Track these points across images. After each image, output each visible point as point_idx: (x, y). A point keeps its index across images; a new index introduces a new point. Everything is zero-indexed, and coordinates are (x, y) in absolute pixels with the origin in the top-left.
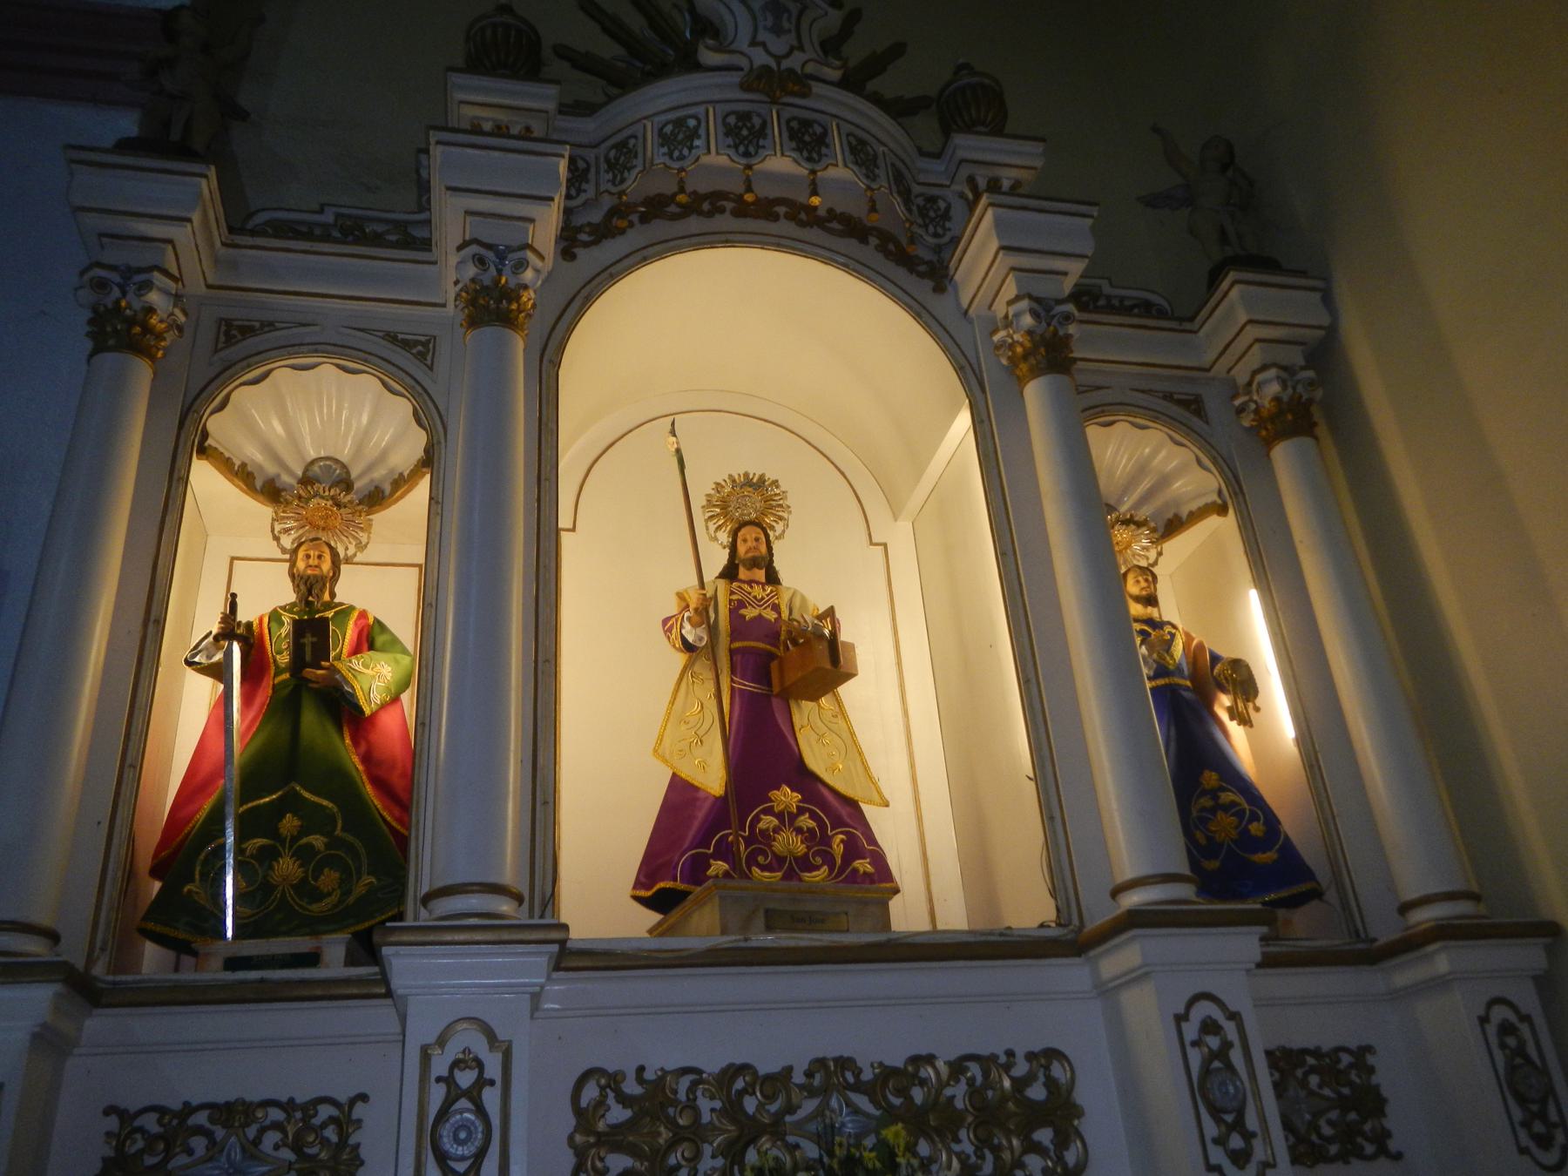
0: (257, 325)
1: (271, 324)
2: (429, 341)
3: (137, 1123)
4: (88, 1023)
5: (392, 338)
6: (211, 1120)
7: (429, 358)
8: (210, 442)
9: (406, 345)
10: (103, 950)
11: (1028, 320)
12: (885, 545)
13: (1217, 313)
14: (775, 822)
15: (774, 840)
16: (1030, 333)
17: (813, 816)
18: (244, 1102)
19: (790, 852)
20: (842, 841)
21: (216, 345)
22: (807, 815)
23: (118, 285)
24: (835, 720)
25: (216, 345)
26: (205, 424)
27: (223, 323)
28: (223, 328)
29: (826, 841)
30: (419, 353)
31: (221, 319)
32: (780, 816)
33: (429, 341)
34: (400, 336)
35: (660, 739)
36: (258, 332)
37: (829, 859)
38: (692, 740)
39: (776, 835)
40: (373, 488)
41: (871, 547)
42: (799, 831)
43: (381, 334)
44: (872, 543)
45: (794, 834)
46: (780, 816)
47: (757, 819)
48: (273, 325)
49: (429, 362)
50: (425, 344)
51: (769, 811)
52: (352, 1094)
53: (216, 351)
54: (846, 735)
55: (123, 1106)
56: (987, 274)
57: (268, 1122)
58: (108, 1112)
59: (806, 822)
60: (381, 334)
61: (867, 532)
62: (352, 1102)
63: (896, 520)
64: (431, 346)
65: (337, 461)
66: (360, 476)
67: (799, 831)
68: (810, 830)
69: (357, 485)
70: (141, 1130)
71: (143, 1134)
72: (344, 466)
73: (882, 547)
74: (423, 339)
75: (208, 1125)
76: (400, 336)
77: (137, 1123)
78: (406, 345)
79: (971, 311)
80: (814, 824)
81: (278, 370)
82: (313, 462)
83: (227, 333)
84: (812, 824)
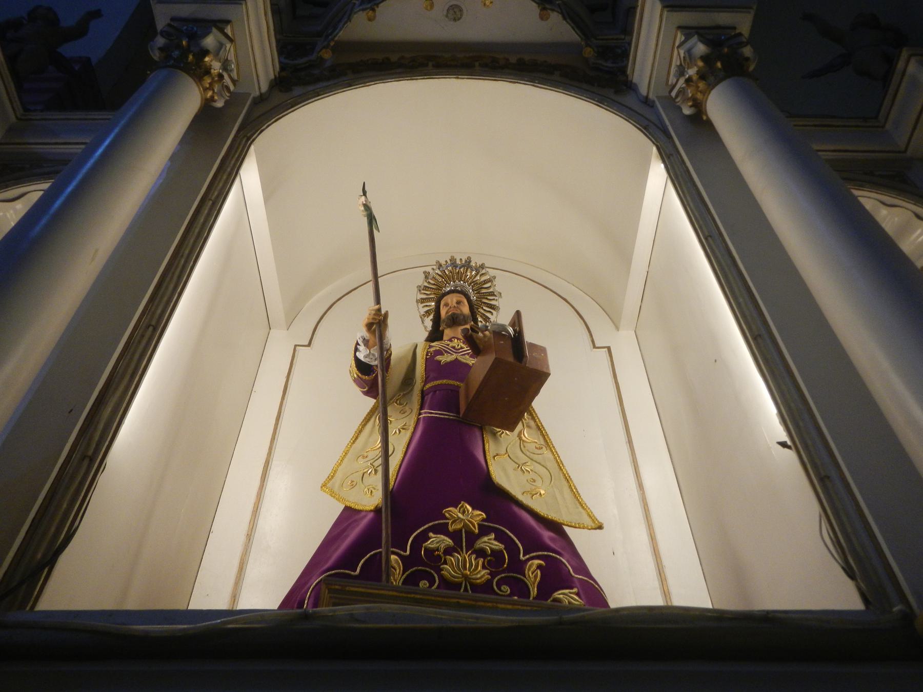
11: (701, 48)
12: (609, 348)
13: (899, 96)
14: (449, 541)
15: (445, 563)
16: (704, 58)
17: (500, 537)
19: (466, 577)
20: (539, 567)
22: (493, 536)
24: (539, 451)
29: (518, 566)
32: (455, 536)
35: (331, 477)
37: (521, 589)
38: (366, 470)
39: (448, 557)
41: (595, 350)
42: (481, 553)
44: (595, 347)
45: (474, 556)
46: (455, 536)
47: (424, 537)
51: (442, 529)
54: (552, 465)
56: (657, 41)
59: (489, 542)
61: (590, 339)
63: (618, 330)
67: (481, 553)
68: (496, 554)
73: (606, 349)
79: (651, 96)
80: (502, 546)
81: (34, 193)
84: (498, 546)
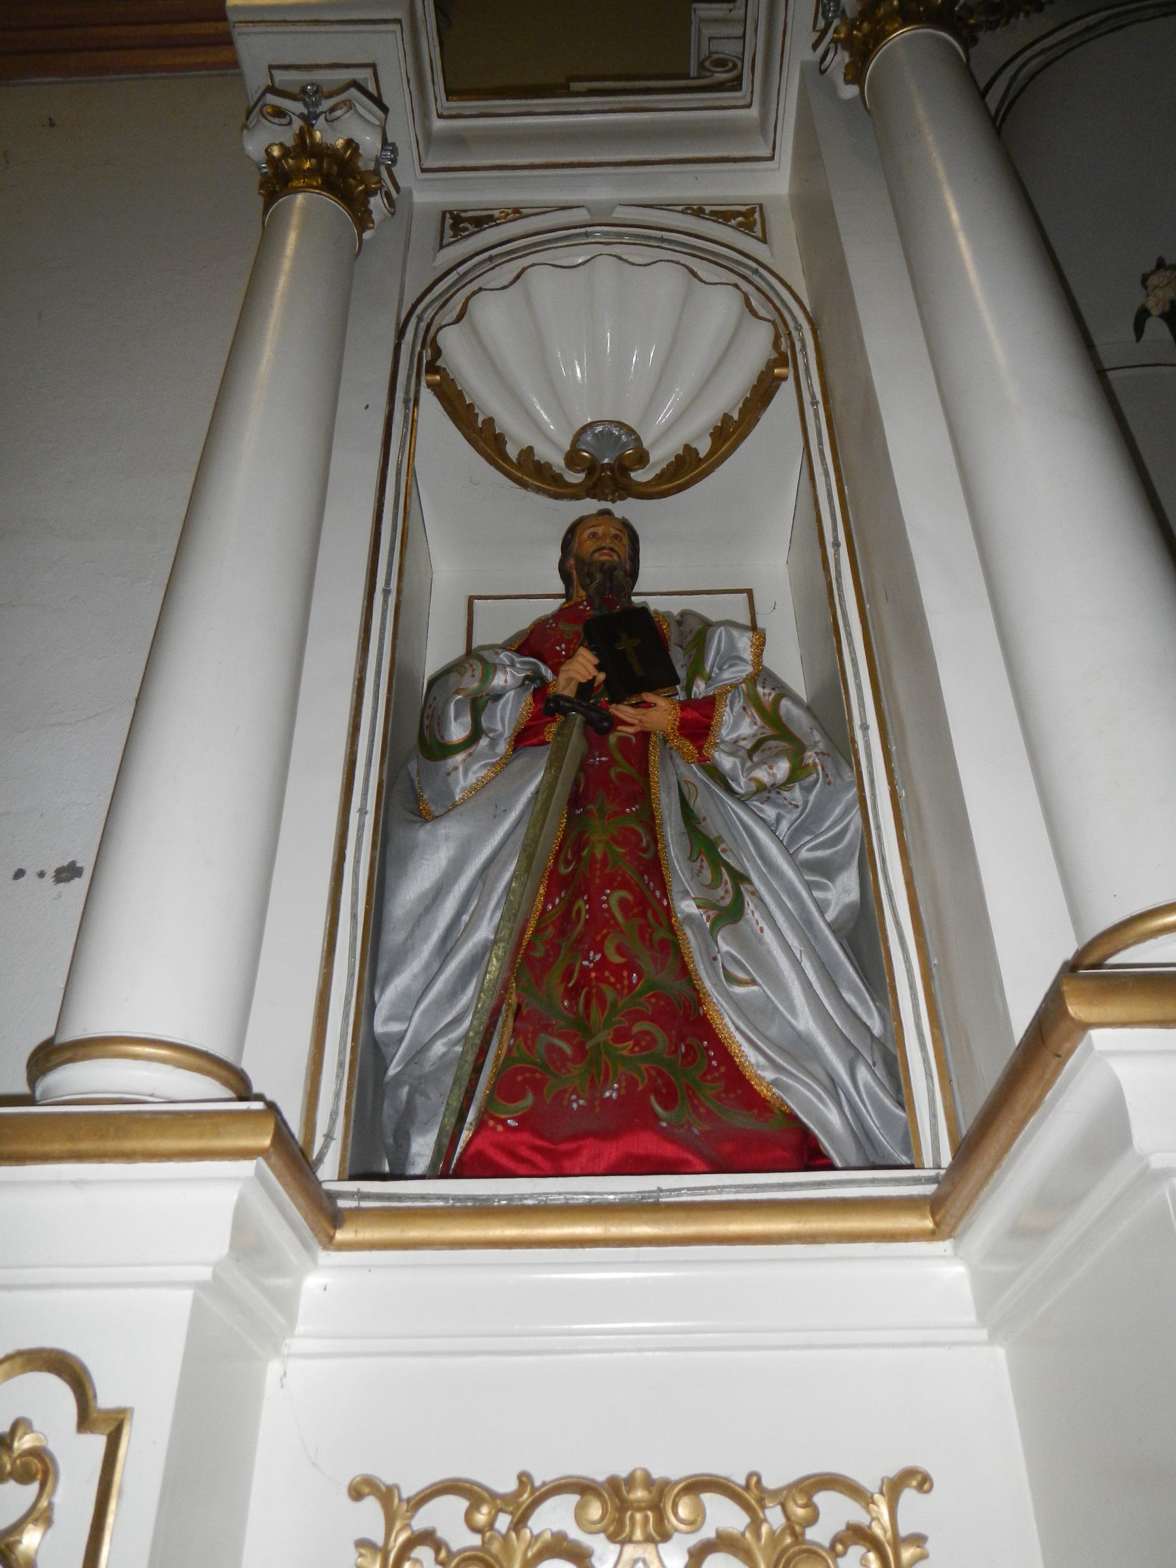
0: (496, 213)
1: (516, 210)
2: (753, 211)
3: (421, 1521)
4: (313, 1282)
5: (698, 211)
6: (579, 1516)
7: (758, 228)
8: (439, 363)
9: (723, 217)
10: (329, 1137)
18: (649, 1482)
21: (442, 238)
23: (301, 116)
25: (442, 238)
26: (434, 340)
27: (448, 215)
28: (449, 221)
30: (740, 224)
31: (444, 213)
33: (753, 211)
34: (708, 209)
36: (498, 222)
40: (681, 452)
43: (680, 208)
48: (519, 212)
49: (759, 234)
50: (750, 213)
52: (892, 1471)
53: (442, 247)
55: (387, 1477)
57: (708, 1532)
58: (356, 1493)
60: (680, 208)
62: (894, 1488)
64: (757, 215)
65: (620, 425)
66: (656, 442)
69: (654, 456)
70: (427, 1537)
71: (437, 1552)
72: (631, 431)
74: (744, 209)
75: (575, 1533)
76: (708, 209)
77: (421, 1521)
78: (723, 217)
82: (584, 429)
83: (455, 227)
